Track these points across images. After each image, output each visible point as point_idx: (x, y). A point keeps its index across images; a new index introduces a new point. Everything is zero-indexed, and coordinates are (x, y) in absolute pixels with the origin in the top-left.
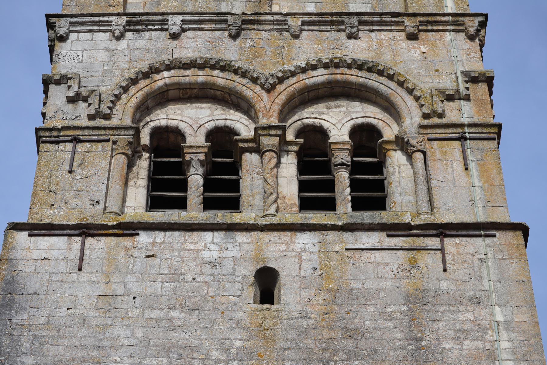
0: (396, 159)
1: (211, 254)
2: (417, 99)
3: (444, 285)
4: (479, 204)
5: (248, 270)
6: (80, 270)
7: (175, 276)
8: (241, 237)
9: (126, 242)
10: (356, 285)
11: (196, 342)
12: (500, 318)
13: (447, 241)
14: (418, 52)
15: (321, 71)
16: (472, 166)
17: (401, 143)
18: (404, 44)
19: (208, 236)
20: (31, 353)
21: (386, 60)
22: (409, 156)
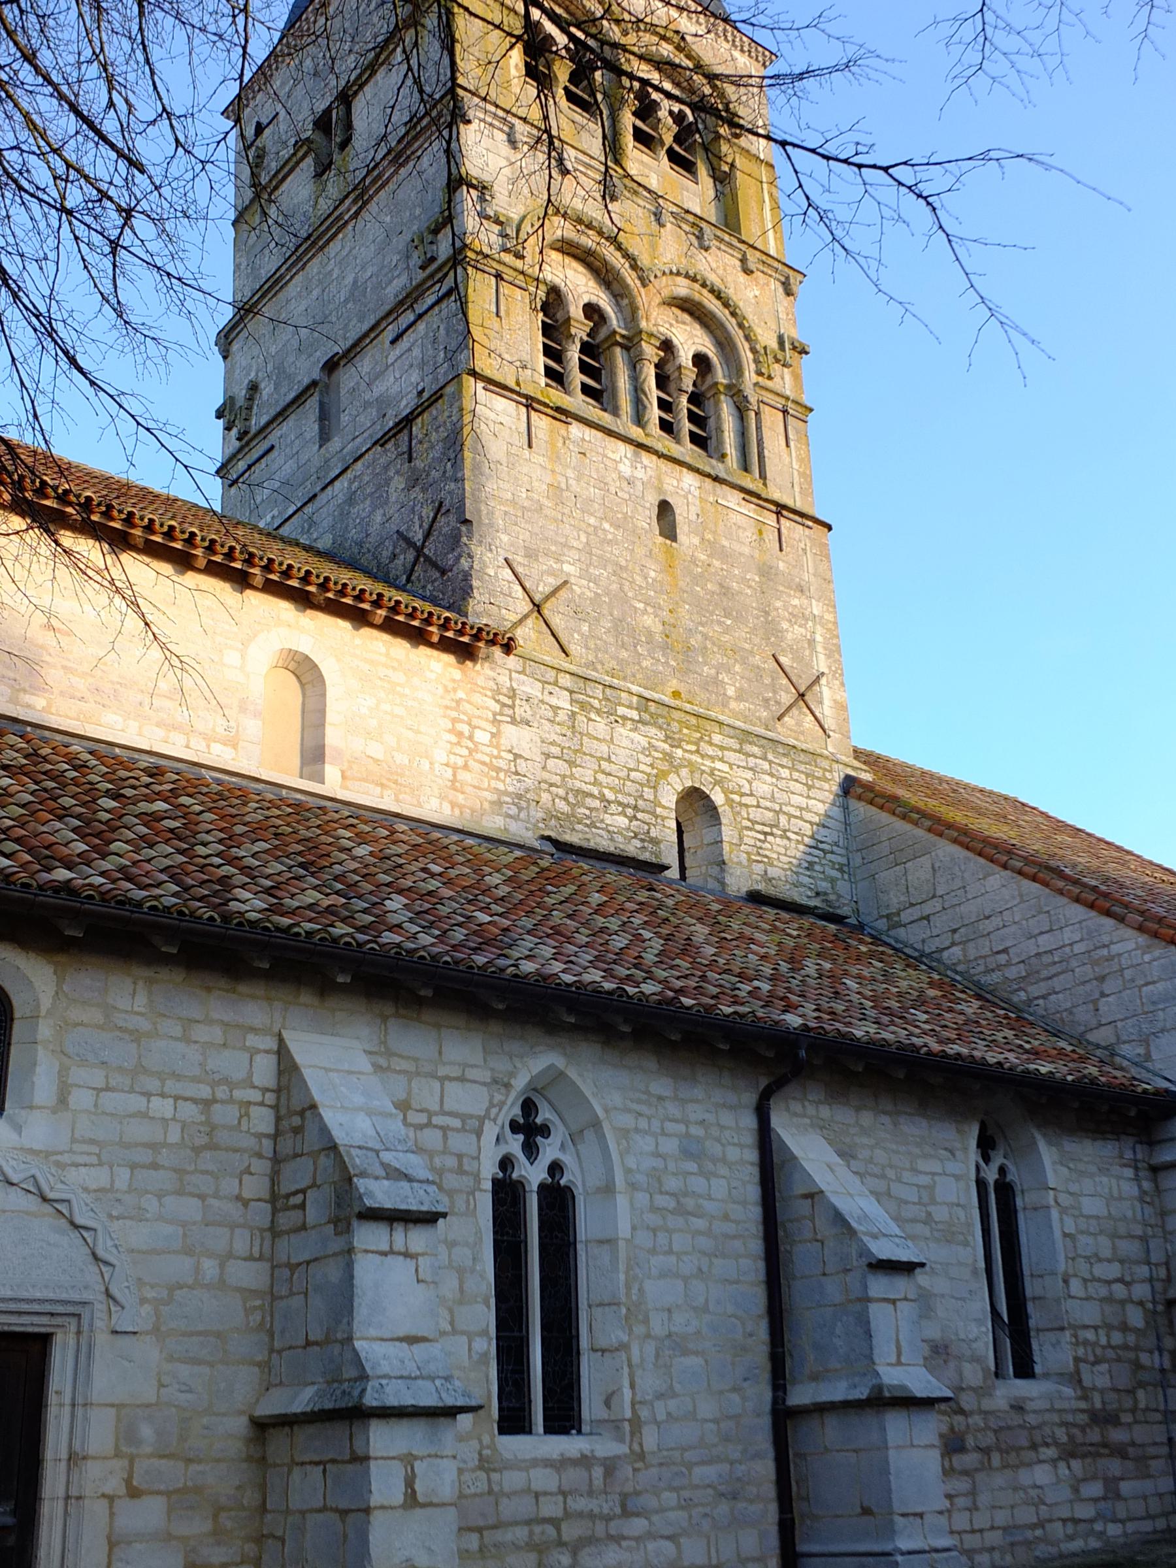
1: (625, 469)
2: (753, 350)
3: (781, 565)
4: (797, 488)
5: (653, 500)
6: (530, 446)
7: (603, 485)
8: (647, 459)
10: (725, 543)
11: (623, 563)
12: (816, 612)
13: (782, 520)
14: (751, 295)
15: (681, 280)
16: (792, 444)
18: (742, 278)
19: (623, 448)
20: (505, 532)
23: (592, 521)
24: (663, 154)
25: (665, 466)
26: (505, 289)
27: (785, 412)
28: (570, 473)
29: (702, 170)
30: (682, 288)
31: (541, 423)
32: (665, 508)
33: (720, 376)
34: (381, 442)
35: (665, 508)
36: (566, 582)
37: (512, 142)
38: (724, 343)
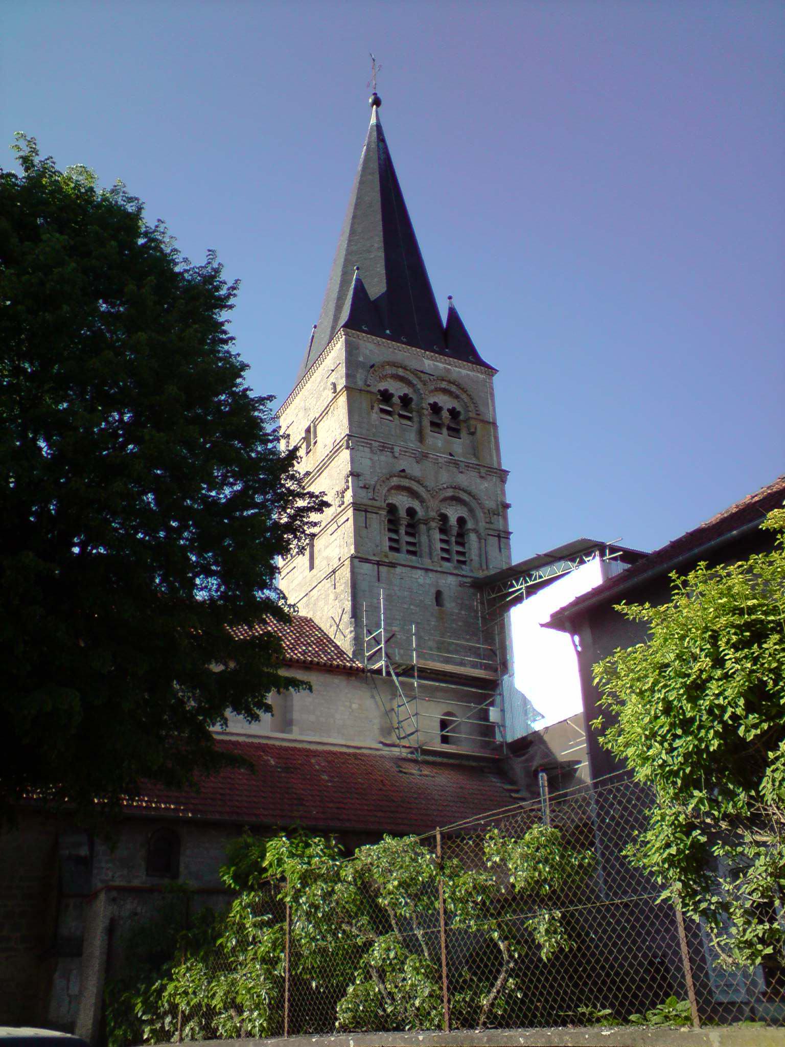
0: (473, 537)
1: (421, 581)
8: (430, 574)
9: (392, 570)
17: (476, 531)
18: (478, 480)
19: (419, 572)
21: (473, 489)
22: (480, 539)
23: (405, 606)
24: (445, 431)
25: (438, 575)
26: (369, 515)
27: (499, 536)
28: (396, 588)
29: (464, 434)
30: (450, 493)
31: (383, 569)
32: (439, 595)
33: (470, 525)
34: (326, 578)
35: (439, 595)
36: (393, 635)
37: (372, 451)
38: (471, 511)
